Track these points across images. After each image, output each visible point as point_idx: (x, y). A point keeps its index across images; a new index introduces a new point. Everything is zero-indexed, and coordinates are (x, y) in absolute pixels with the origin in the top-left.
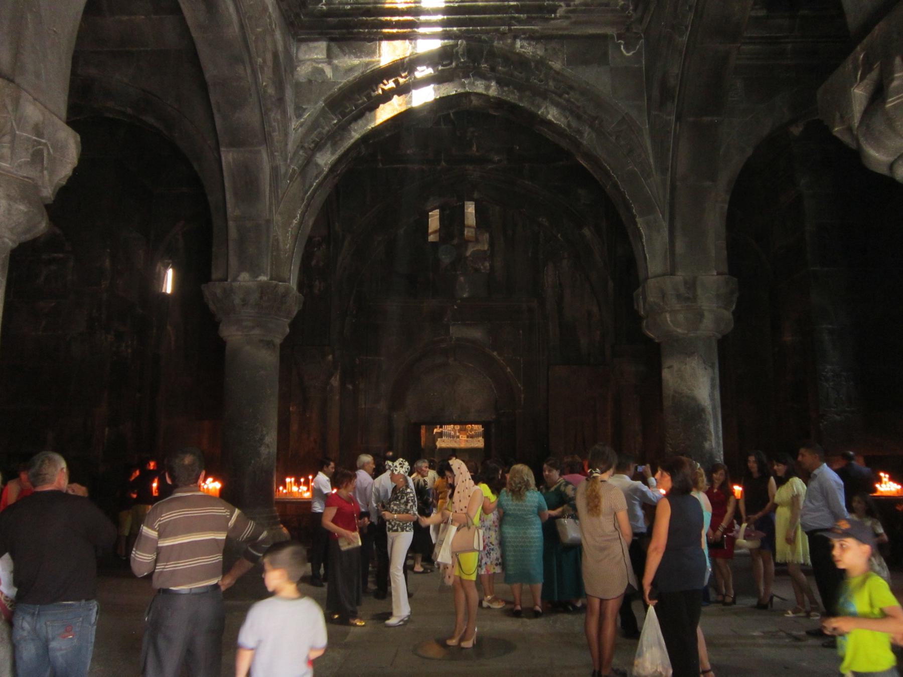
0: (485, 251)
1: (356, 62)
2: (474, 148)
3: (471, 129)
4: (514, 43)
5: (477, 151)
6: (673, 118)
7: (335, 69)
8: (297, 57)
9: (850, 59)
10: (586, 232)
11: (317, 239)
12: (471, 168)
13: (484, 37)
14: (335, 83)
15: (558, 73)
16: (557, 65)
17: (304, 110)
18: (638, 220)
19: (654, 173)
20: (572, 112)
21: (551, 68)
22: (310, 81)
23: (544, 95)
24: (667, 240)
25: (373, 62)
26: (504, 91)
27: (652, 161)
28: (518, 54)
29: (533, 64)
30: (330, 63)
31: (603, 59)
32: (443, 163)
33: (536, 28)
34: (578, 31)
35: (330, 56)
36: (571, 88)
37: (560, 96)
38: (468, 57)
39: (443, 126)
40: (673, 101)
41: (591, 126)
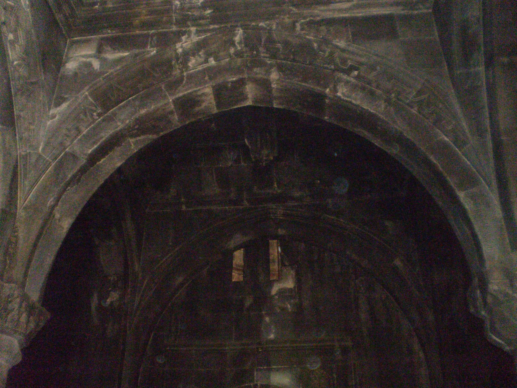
0: (290, 290)
1: (126, 54)
3: (265, 152)
5: (279, 188)
6: (481, 69)
7: (104, 61)
8: (66, 55)
10: (398, 262)
14: (101, 73)
15: (343, 50)
16: (342, 44)
17: (64, 100)
18: (461, 195)
20: (363, 89)
21: (337, 47)
22: (76, 74)
24: (499, 213)
27: (464, 124)
28: (299, 36)
29: (315, 45)
32: (246, 203)
34: (360, 14)
35: (100, 50)
36: (361, 64)
38: (246, 46)
41: (388, 101)
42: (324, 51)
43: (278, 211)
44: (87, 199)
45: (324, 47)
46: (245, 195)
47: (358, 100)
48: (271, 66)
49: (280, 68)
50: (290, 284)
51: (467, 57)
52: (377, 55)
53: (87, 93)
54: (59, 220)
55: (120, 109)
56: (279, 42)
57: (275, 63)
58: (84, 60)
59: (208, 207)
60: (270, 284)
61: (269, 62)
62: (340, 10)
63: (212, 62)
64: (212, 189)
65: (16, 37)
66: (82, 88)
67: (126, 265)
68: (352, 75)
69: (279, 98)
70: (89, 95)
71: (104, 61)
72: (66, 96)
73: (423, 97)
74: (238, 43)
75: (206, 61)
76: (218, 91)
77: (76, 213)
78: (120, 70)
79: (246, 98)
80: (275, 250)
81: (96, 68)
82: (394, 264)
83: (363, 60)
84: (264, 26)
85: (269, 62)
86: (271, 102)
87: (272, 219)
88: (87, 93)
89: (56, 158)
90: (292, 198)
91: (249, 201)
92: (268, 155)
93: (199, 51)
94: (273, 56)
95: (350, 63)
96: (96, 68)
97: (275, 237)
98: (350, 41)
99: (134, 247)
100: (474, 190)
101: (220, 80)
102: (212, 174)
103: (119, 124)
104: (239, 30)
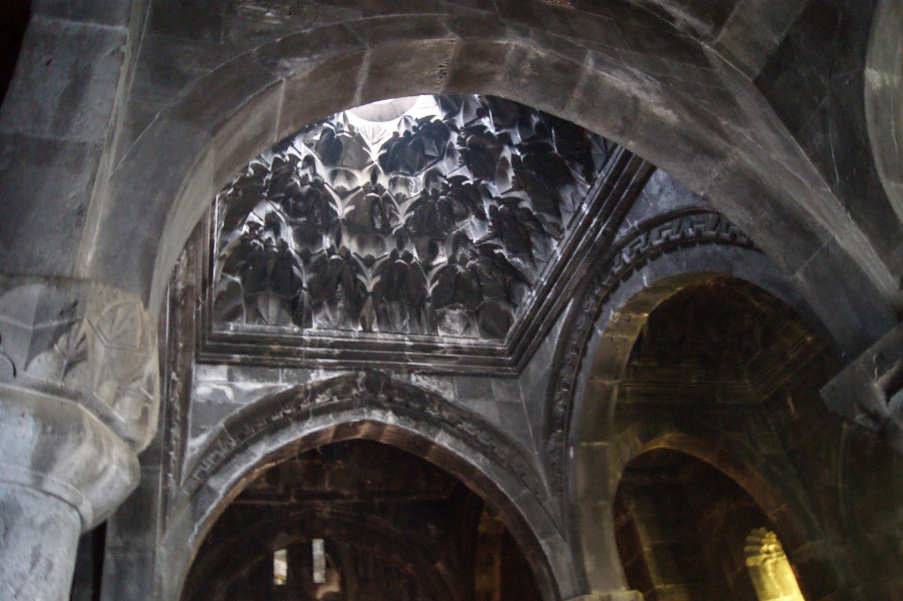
2: (327, 483)
3: (339, 462)
4: (409, 378)
7: (237, 391)
8: (196, 378)
9: (861, 359)
10: (440, 566)
13: (382, 370)
17: (203, 431)
18: (542, 542)
19: (549, 495)
21: (445, 401)
23: (438, 424)
25: (275, 387)
28: (415, 387)
29: (427, 396)
30: (231, 386)
31: (488, 394)
33: (429, 365)
37: (453, 426)
38: (368, 388)
41: (485, 454)
42: (434, 403)
43: (325, 510)
46: (293, 491)
47: (462, 452)
49: (397, 412)
50: (334, 588)
58: (215, 386)
60: (316, 586)
63: (336, 400)
71: (237, 391)
72: (203, 427)
75: (331, 400)
80: (318, 547)
90: (342, 497)
93: (326, 389)
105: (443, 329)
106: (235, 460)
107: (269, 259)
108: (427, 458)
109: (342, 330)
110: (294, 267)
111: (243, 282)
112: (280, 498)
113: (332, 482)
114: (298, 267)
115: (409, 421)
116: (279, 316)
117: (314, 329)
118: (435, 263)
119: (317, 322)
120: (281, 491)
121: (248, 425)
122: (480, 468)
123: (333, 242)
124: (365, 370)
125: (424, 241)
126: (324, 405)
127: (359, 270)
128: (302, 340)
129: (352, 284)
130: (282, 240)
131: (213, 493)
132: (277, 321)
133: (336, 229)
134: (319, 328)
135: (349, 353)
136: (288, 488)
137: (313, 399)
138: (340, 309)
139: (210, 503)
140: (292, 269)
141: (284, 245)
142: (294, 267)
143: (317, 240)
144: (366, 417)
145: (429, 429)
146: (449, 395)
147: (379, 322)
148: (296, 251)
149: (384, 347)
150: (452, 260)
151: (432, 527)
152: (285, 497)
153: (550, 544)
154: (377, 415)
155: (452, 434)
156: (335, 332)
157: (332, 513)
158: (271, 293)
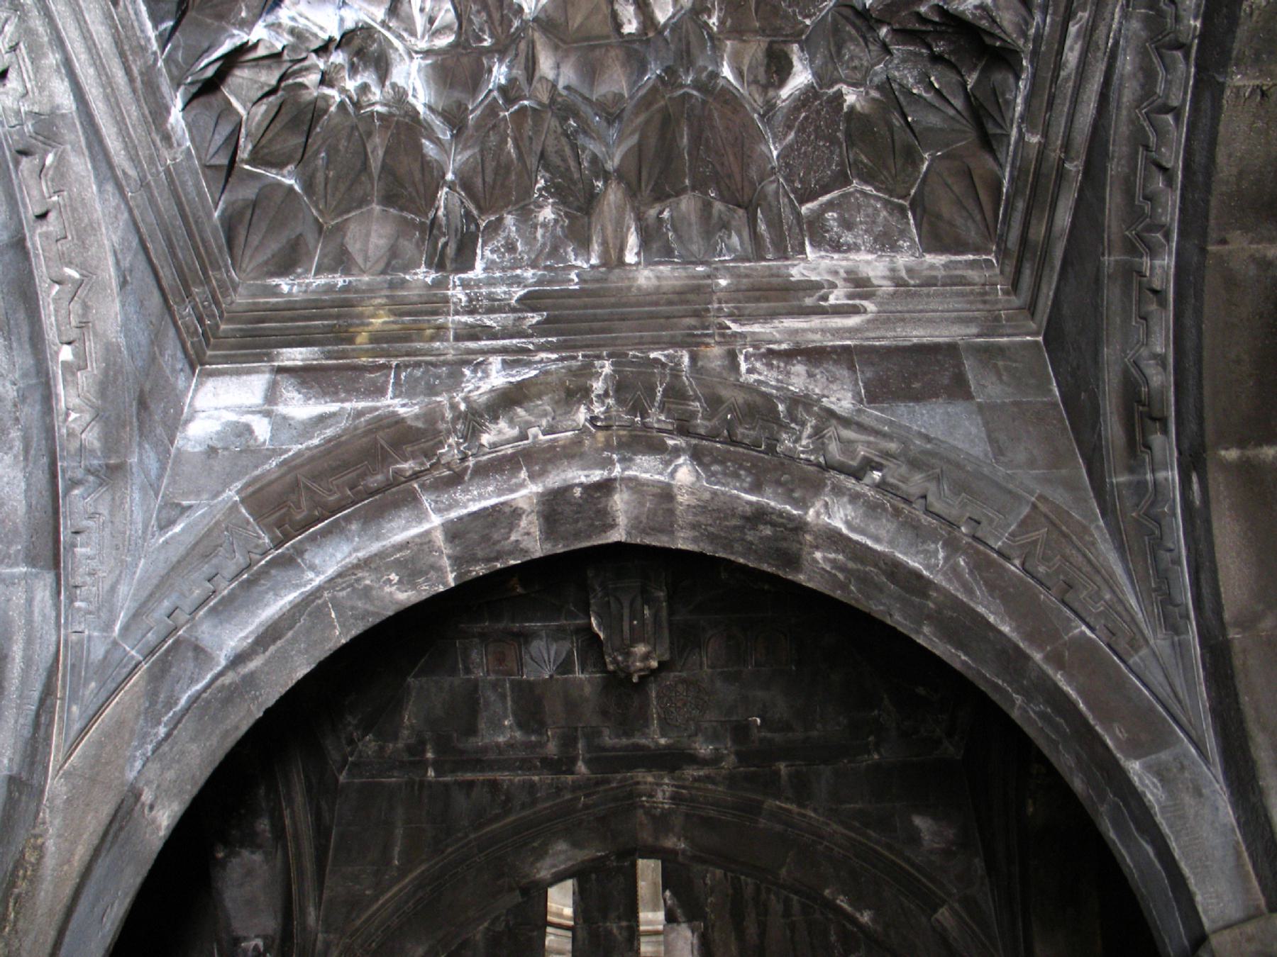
3: (641, 649)
6: (1172, 475)
7: (280, 424)
8: (191, 405)
11: (253, 943)
12: (650, 779)
14: (275, 452)
15: (845, 422)
18: (1134, 767)
19: (1148, 632)
21: (831, 413)
22: (212, 451)
25: (377, 409)
26: (714, 474)
27: (1133, 602)
29: (781, 407)
30: (268, 414)
31: (959, 389)
32: (581, 767)
36: (887, 455)
37: (857, 474)
38: (619, 401)
39: (579, 675)
40: (1165, 431)
42: (803, 424)
43: (660, 790)
44: (220, 755)
45: (801, 413)
47: (880, 539)
48: (677, 451)
49: (697, 456)
51: (1136, 446)
52: (928, 439)
53: (237, 498)
54: (152, 807)
55: (312, 538)
56: (697, 398)
57: (684, 445)
58: (233, 417)
59: (489, 775)
61: (671, 442)
62: (837, 332)
64: (503, 731)
65: (81, 356)
66: (226, 485)
67: (288, 913)
68: (867, 480)
69: (694, 526)
70: (243, 501)
71: (280, 424)
73: (1034, 535)
74: (598, 396)
76: (554, 507)
77: (191, 790)
78: (317, 447)
79: (613, 526)
81: (261, 439)
82: (937, 920)
83: (893, 446)
84: (663, 359)
85: (671, 442)
86: (670, 532)
87: (643, 807)
88: (237, 498)
89: (152, 652)
90: (694, 760)
91: (588, 762)
92: (646, 657)
94: (683, 429)
95: (862, 452)
96: (261, 439)
97: (650, 853)
98: (861, 402)
99: (309, 866)
100: (1164, 756)
101: (555, 480)
102: (503, 697)
103: (311, 575)
104: (602, 367)
105: (817, 244)
106: (265, 583)
107: (370, 134)
108: (801, 578)
109: (546, 268)
110: (426, 142)
111: (309, 186)
112: (551, 765)
113: (665, 727)
114: (437, 141)
115: (736, 476)
116: (393, 252)
117: (478, 272)
118: (785, 92)
119: (484, 255)
120: (552, 748)
121: (300, 501)
122: (938, 579)
123: (518, 72)
124: (610, 356)
125: (755, 49)
126: (508, 450)
127: (585, 129)
128: (446, 300)
129: (572, 163)
130: (394, 86)
131: (201, 653)
132: (388, 264)
133: (523, 45)
134: (485, 270)
135: (568, 318)
136: (568, 741)
137: (472, 433)
138: (544, 225)
139: (193, 681)
140: (420, 147)
141: (400, 96)
142: (426, 142)
143: (477, 77)
144: (617, 471)
145: (793, 490)
146: (842, 400)
147: (645, 244)
148: (430, 108)
149: (654, 297)
150: (823, 78)
151: (918, 821)
152: (564, 764)
153: (1161, 774)
154: (646, 468)
155: (855, 498)
156: (529, 274)
157: (675, 798)
158: (377, 208)
